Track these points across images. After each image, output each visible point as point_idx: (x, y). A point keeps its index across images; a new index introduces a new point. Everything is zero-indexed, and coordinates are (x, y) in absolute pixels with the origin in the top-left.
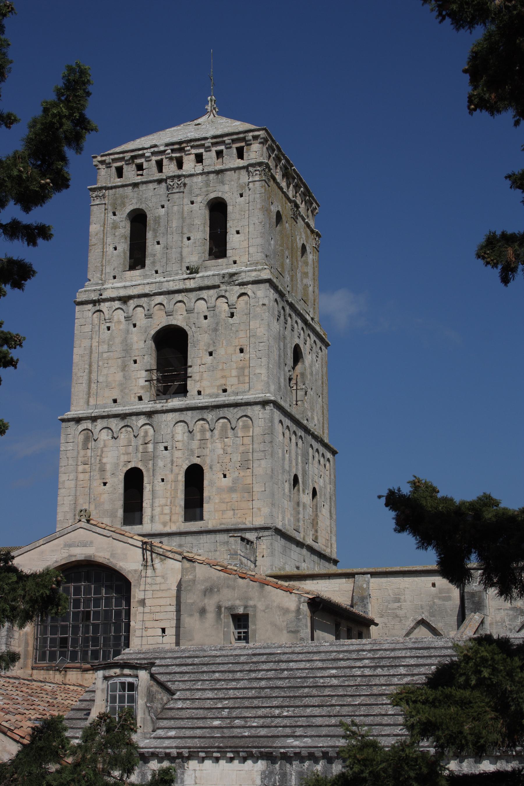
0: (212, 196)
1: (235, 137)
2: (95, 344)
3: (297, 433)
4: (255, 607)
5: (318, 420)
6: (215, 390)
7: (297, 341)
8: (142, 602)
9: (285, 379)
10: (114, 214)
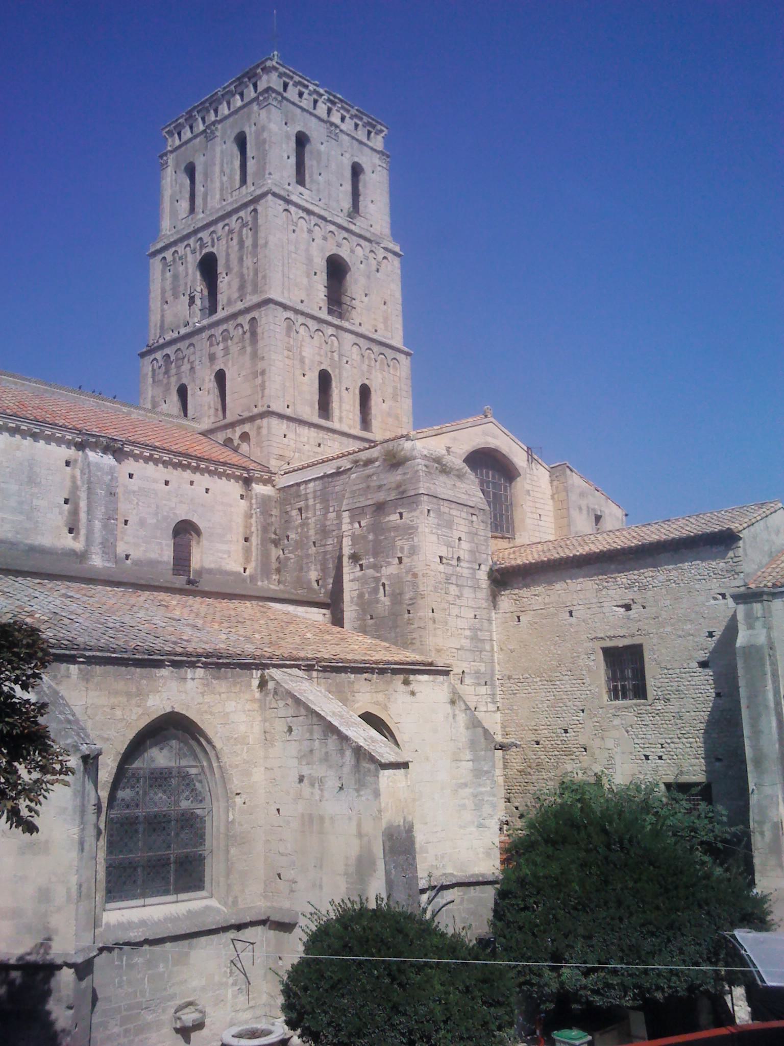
0: (356, 159)
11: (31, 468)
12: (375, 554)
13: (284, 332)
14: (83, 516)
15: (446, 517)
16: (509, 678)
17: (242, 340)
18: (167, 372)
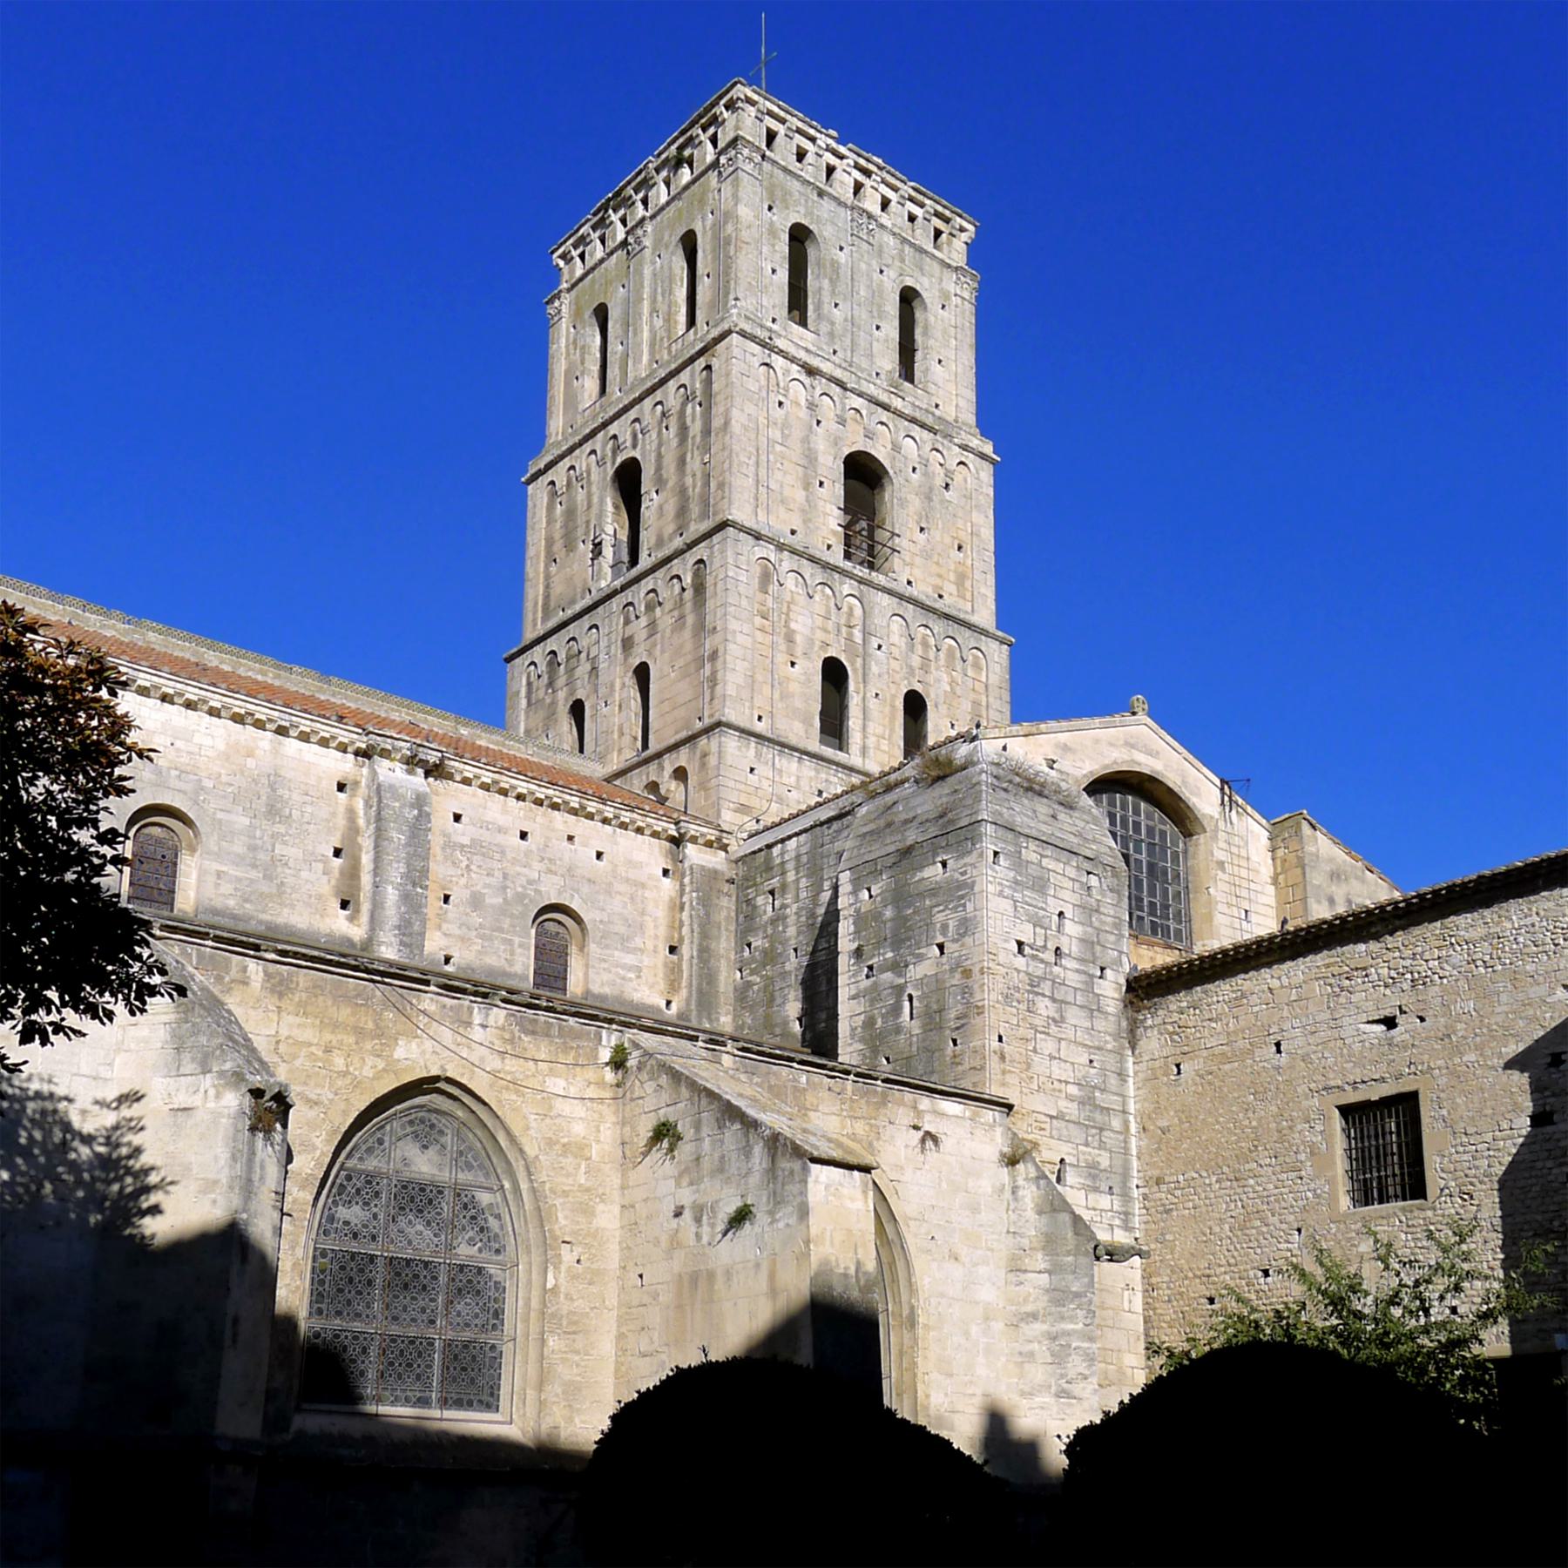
6: (930, 591)
11: (274, 790)
12: (897, 944)
13: (756, 582)
14: (366, 879)
15: (1032, 870)
16: (1159, 1181)
17: (680, 603)
18: (550, 684)
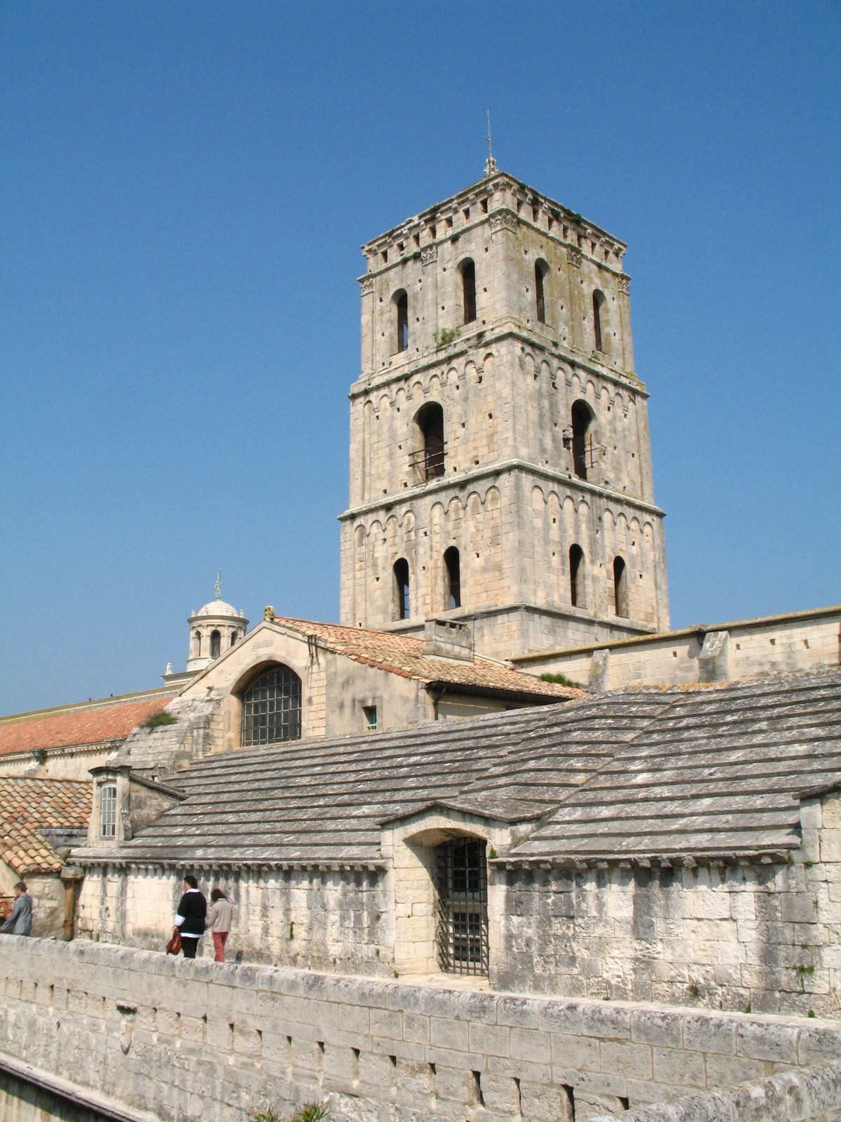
0: (462, 257)
1: (477, 191)
2: (367, 436)
3: (575, 497)
4: (381, 697)
5: (632, 481)
7: (580, 396)
8: (310, 700)
9: (554, 440)
10: (381, 300)
